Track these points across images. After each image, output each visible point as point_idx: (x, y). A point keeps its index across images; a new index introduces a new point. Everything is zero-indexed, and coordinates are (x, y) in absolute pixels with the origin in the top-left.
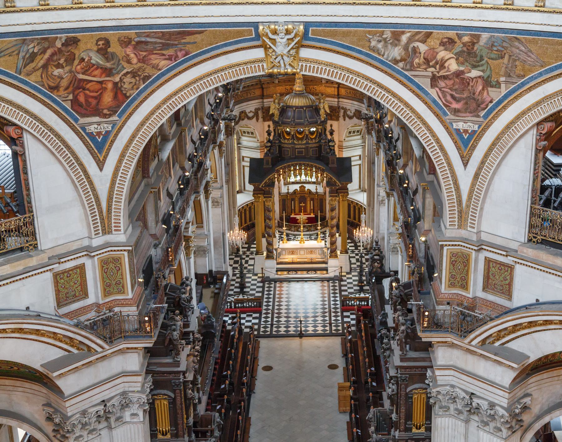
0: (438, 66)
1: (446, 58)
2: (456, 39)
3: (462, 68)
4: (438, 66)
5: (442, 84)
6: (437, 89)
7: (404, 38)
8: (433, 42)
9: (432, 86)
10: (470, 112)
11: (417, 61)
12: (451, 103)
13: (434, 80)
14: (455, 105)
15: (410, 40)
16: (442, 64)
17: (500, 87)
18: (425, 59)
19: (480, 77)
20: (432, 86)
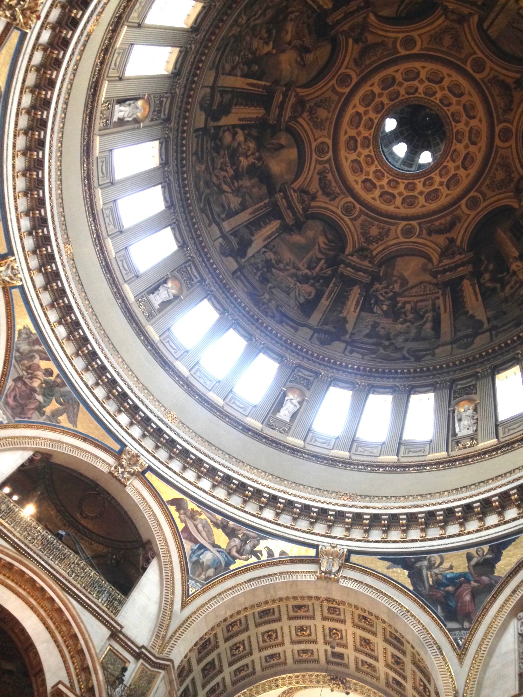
0: (30, 376)
1: (40, 377)
2: (55, 375)
3: (38, 389)
4: (30, 376)
5: (19, 384)
6: (14, 384)
7: (37, 347)
8: (44, 364)
9: (15, 380)
10: (13, 412)
11: (26, 362)
12: (10, 397)
13: (19, 379)
14: (10, 401)
15: (38, 351)
16: (33, 377)
17: (42, 416)
18: (30, 366)
19: (40, 402)
20: (15, 380)
